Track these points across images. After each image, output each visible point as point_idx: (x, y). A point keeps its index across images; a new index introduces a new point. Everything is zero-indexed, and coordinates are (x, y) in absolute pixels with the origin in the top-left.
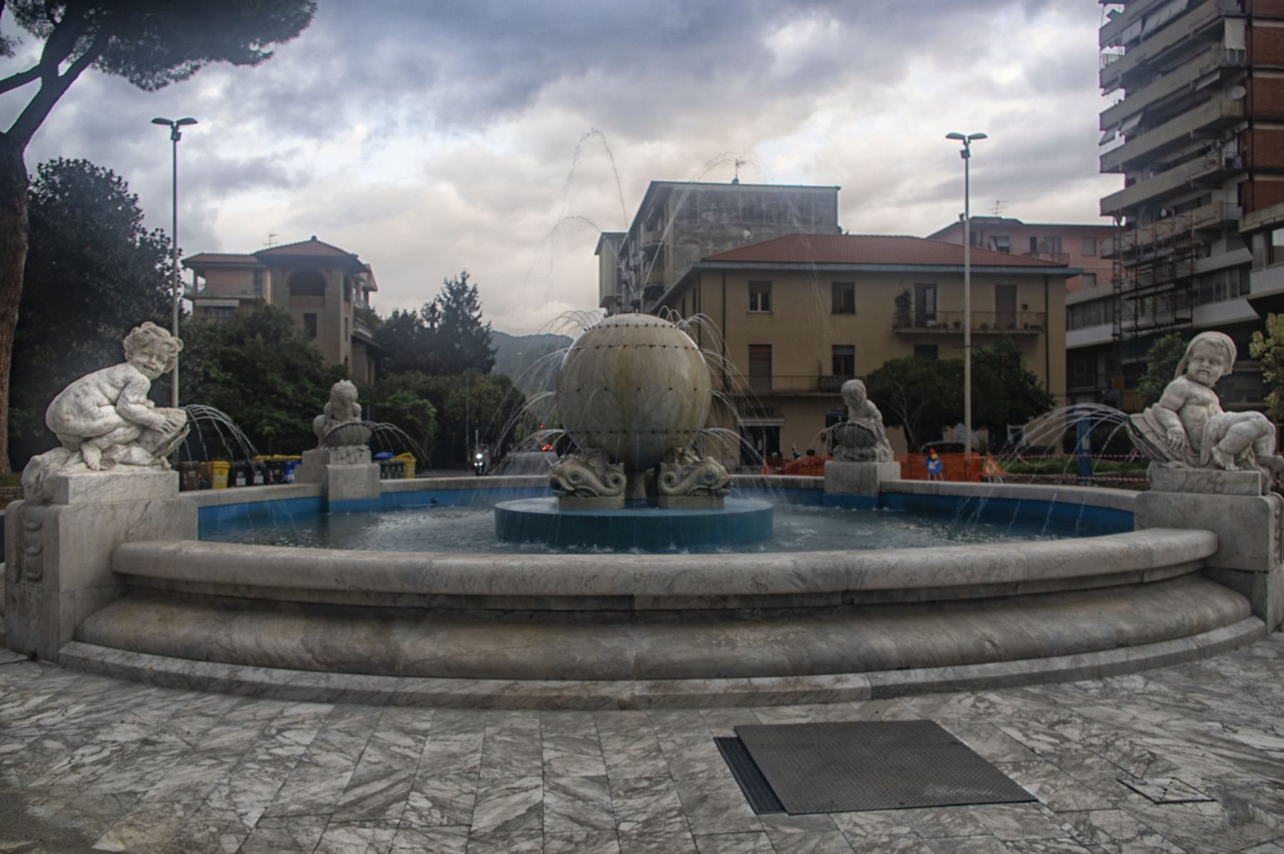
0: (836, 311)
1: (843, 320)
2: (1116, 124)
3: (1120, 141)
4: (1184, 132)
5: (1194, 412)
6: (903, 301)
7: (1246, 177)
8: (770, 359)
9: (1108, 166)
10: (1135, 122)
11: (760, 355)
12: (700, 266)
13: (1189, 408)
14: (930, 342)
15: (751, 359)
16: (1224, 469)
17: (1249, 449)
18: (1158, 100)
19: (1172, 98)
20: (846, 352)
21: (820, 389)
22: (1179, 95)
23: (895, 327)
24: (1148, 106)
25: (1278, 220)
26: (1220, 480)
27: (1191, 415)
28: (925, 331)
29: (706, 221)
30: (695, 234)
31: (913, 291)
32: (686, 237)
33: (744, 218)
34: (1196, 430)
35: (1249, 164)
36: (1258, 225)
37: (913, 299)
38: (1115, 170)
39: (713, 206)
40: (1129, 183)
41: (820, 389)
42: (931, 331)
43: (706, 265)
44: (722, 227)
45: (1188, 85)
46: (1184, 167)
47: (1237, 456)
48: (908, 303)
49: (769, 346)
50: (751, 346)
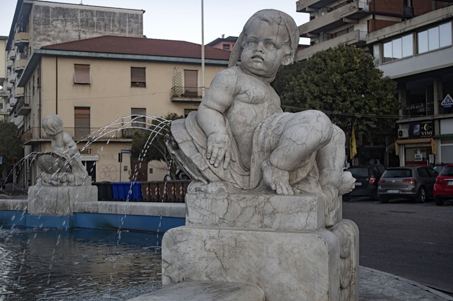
1: (138, 90)
5: (242, 111)
7: (371, 17)
8: (89, 118)
11: (82, 113)
12: (39, 52)
13: (238, 107)
15: (75, 118)
16: (275, 192)
17: (311, 162)
21: (123, 137)
25: (386, 36)
26: (269, 208)
27: (241, 118)
29: (56, 27)
30: (49, 35)
32: (42, 37)
33: (82, 26)
34: (245, 139)
35: (372, 10)
36: (376, 40)
38: (303, 11)
39: (61, 17)
40: (312, 18)
41: (123, 137)
43: (44, 52)
44: (67, 31)
46: (340, 10)
47: (292, 171)
49: (89, 108)
50: (76, 108)
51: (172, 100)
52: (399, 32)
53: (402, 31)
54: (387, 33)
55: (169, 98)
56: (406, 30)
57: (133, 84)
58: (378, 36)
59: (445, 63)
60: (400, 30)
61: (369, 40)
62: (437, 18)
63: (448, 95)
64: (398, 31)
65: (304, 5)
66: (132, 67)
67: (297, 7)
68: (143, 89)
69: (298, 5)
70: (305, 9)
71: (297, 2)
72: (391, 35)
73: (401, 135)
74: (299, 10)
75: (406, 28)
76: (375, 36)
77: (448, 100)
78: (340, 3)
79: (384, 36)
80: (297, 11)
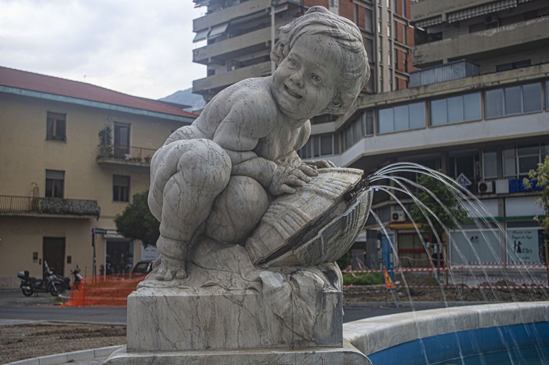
0: (50, 137)
1: (55, 146)
2: (207, 29)
3: (204, 43)
4: (262, 42)
6: (104, 135)
9: (198, 57)
10: (223, 29)
14: (125, 173)
18: (240, 17)
19: (251, 17)
20: (59, 177)
21: (34, 208)
22: (255, 16)
23: (99, 158)
24: (232, 20)
28: (124, 163)
31: (112, 128)
37: (112, 134)
40: (210, 73)
42: (129, 163)
45: (264, 10)
48: (109, 137)
51: (100, 161)
52: (409, 99)
53: (413, 98)
54: (391, 98)
55: (95, 158)
56: (418, 97)
57: (50, 137)
58: (376, 101)
59: (456, 140)
60: (411, 97)
61: (362, 105)
62: (464, 87)
63: (462, 175)
64: (406, 98)
65: (205, 54)
66: (48, 112)
67: (194, 56)
68: (62, 144)
69: (196, 53)
70: (207, 59)
71: (194, 51)
72: (396, 101)
73: (397, 218)
74: (198, 60)
75: (419, 95)
76: (372, 101)
77: (462, 180)
78: (255, 57)
79: (386, 101)
80: (194, 61)
